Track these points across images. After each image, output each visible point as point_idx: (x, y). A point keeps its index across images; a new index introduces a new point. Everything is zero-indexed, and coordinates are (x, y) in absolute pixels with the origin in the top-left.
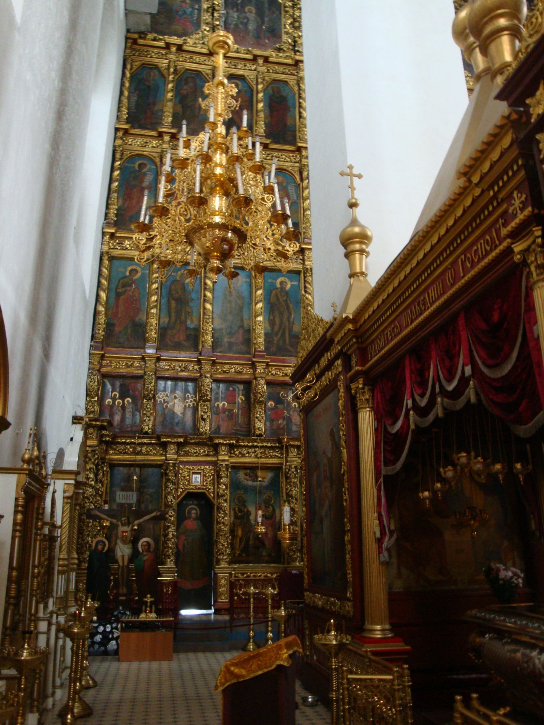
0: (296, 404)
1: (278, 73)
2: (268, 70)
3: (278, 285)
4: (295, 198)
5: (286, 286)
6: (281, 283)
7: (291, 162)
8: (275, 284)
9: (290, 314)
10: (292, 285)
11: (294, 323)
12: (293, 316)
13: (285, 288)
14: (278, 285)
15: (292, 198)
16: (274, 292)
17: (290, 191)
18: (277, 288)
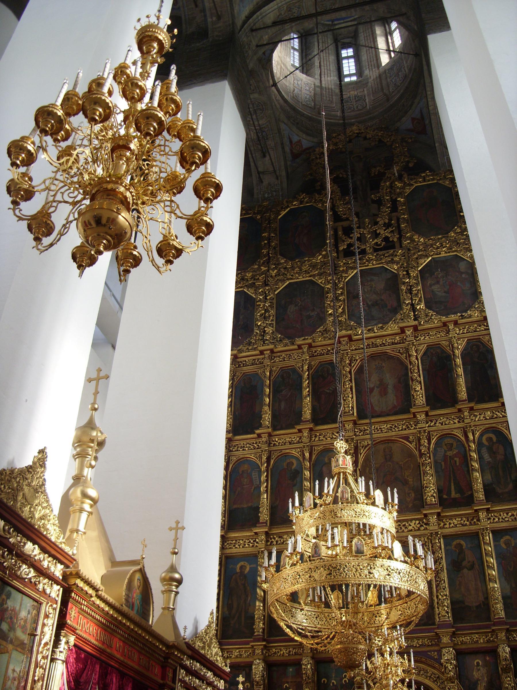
0: (248, 684)
1: (248, 366)
2: (239, 365)
3: (238, 570)
4: (258, 483)
5: (245, 569)
6: (241, 567)
7: (255, 449)
8: (236, 569)
9: (247, 596)
10: (250, 568)
11: (250, 605)
12: (249, 598)
13: (244, 572)
14: (238, 570)
15: (255, 484)
16: (234, 577)
17: (253, 476)
18: (237, 573)
